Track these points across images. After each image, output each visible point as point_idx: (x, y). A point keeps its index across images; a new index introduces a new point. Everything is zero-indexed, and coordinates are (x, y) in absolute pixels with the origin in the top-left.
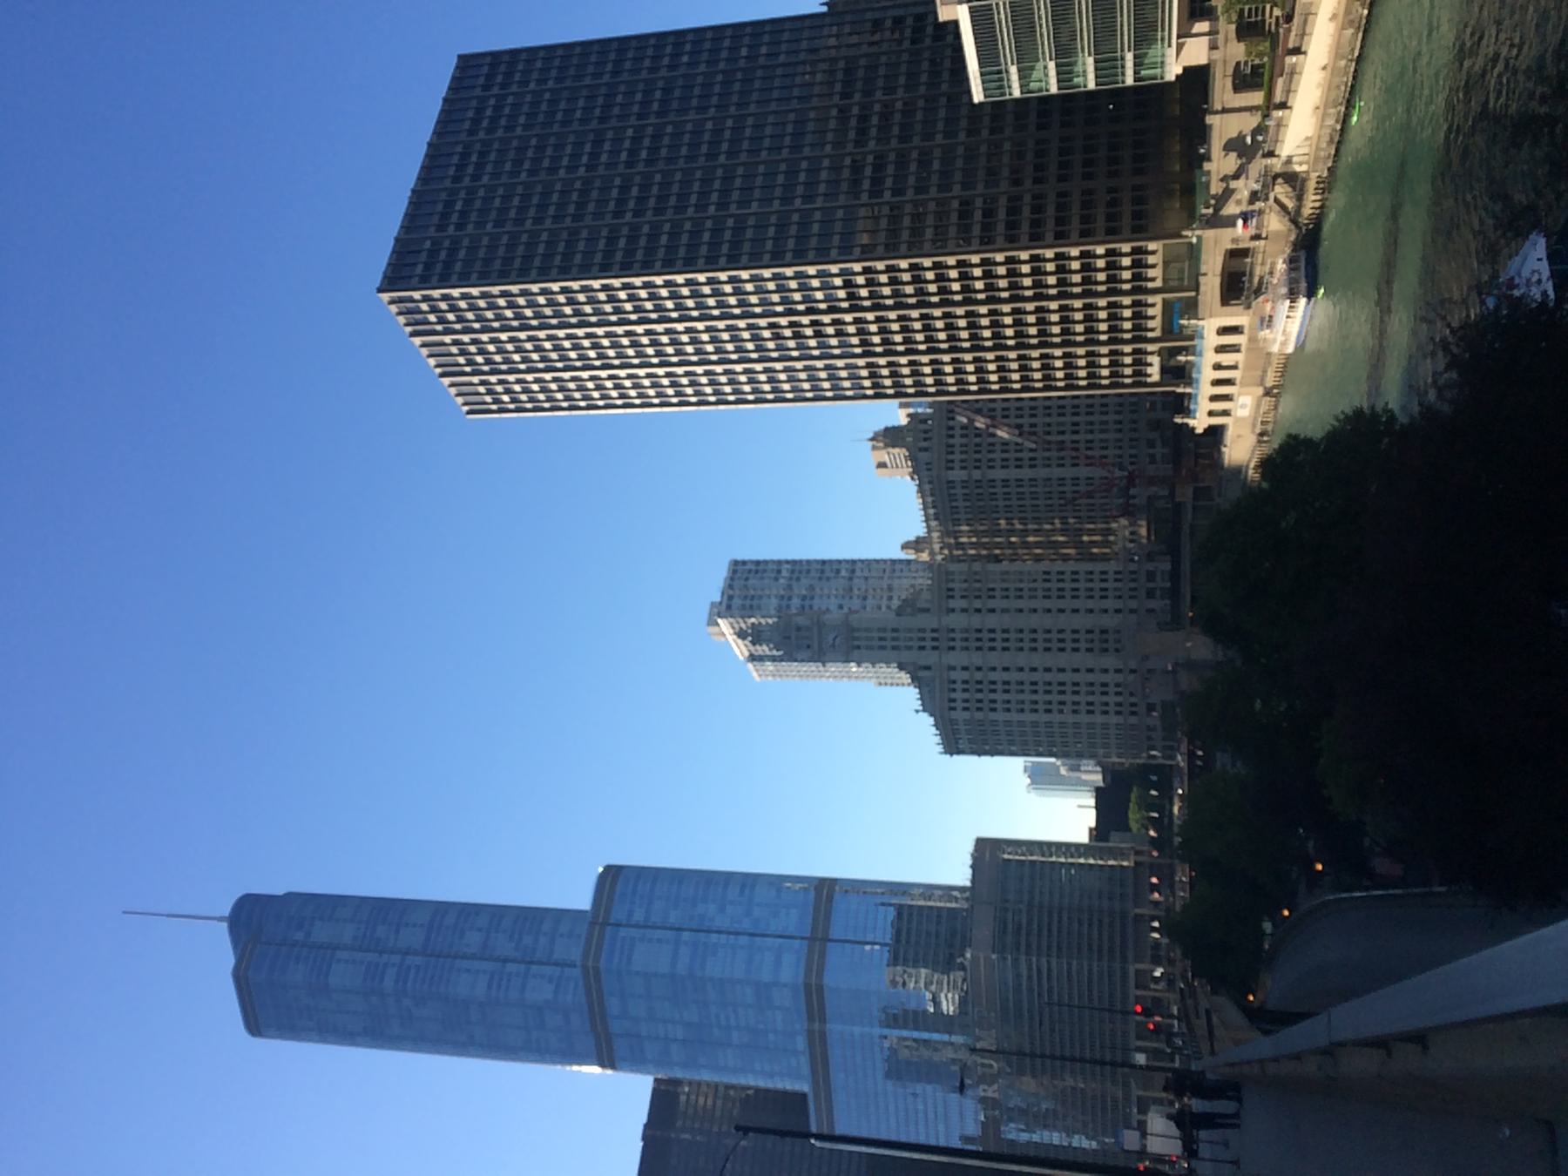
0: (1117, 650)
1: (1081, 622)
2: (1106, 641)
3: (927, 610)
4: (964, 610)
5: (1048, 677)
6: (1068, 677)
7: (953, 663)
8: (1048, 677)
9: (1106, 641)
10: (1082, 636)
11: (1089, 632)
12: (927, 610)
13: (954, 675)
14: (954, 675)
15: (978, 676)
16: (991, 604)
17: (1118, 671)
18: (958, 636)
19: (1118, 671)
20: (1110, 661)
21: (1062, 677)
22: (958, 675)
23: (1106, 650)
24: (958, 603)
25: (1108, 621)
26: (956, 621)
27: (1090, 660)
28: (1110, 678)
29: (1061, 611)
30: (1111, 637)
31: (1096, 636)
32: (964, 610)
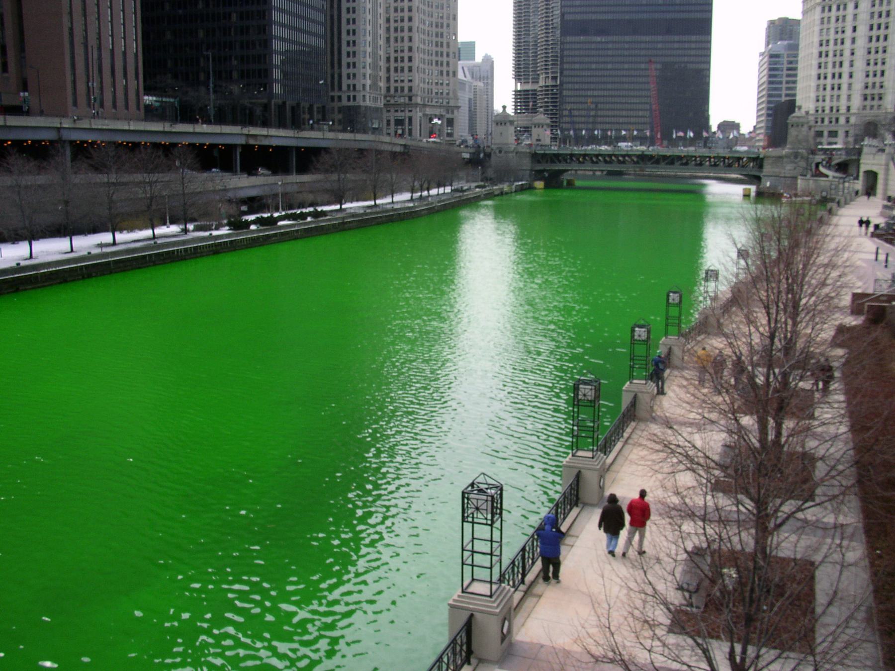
0: (864, 107)
2: (873, 99)
5: (847, 53)
6: (846, 69)
8: (847, 53)
9: (873, 99)
10: (878, 80)
17: (848, 109)
19: (848, 109)
20: (856, 102)
21: (846, 64)
23: (866, 99)
27: (858, 86)
28: (843, 104)
30: (875, 103)
31: (876, 91)
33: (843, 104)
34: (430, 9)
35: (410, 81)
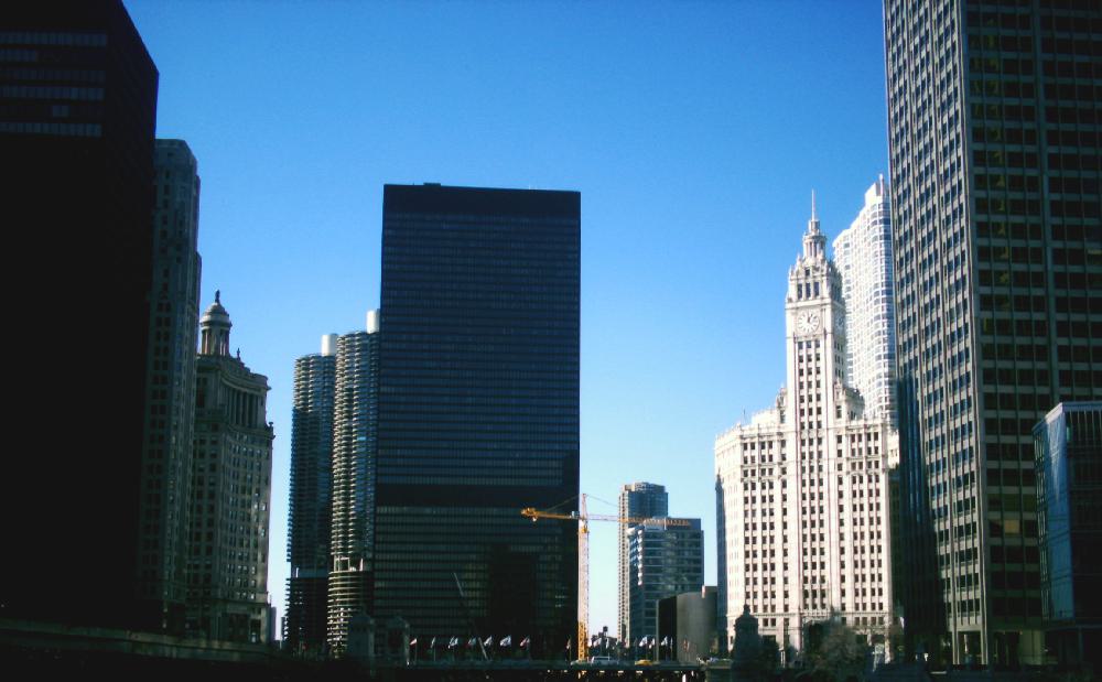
1: (831, 573)
3: (839, 415)
4: (840, 453)
7: (787, 444)
11: (823, 580)
12: (839, 415)
13: (776, 445)
14: (776, 445)
15: (777, 471)
16: (847, 480)
17: (786, 608)
18: (814, 448)
19: (786, 608)
20: (795, 600)
22: (775, 451)
24: (845, 446)
25: (834, 599)
26: (829, 447)
29: (842, 551)
32: (840, 453)
33: (779, 601)
34: (236, 469)
35: (208, 567)
